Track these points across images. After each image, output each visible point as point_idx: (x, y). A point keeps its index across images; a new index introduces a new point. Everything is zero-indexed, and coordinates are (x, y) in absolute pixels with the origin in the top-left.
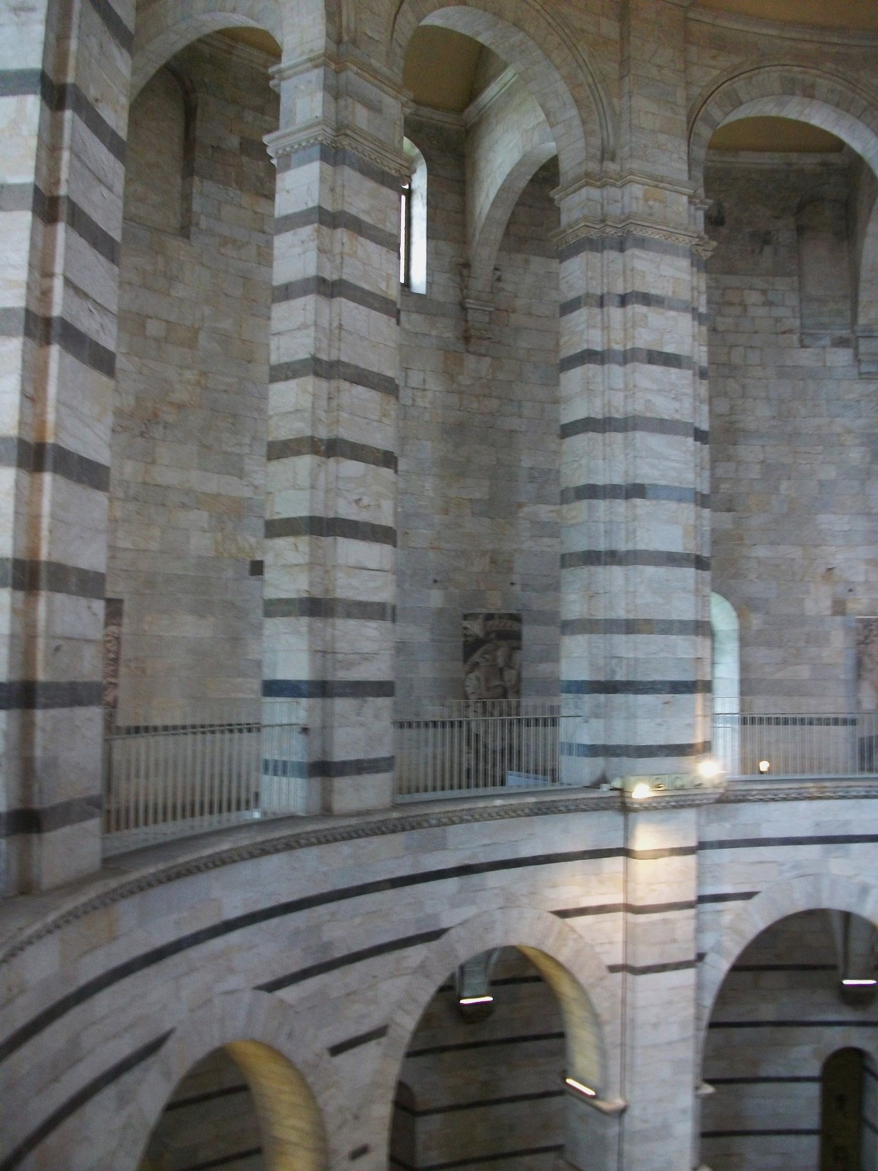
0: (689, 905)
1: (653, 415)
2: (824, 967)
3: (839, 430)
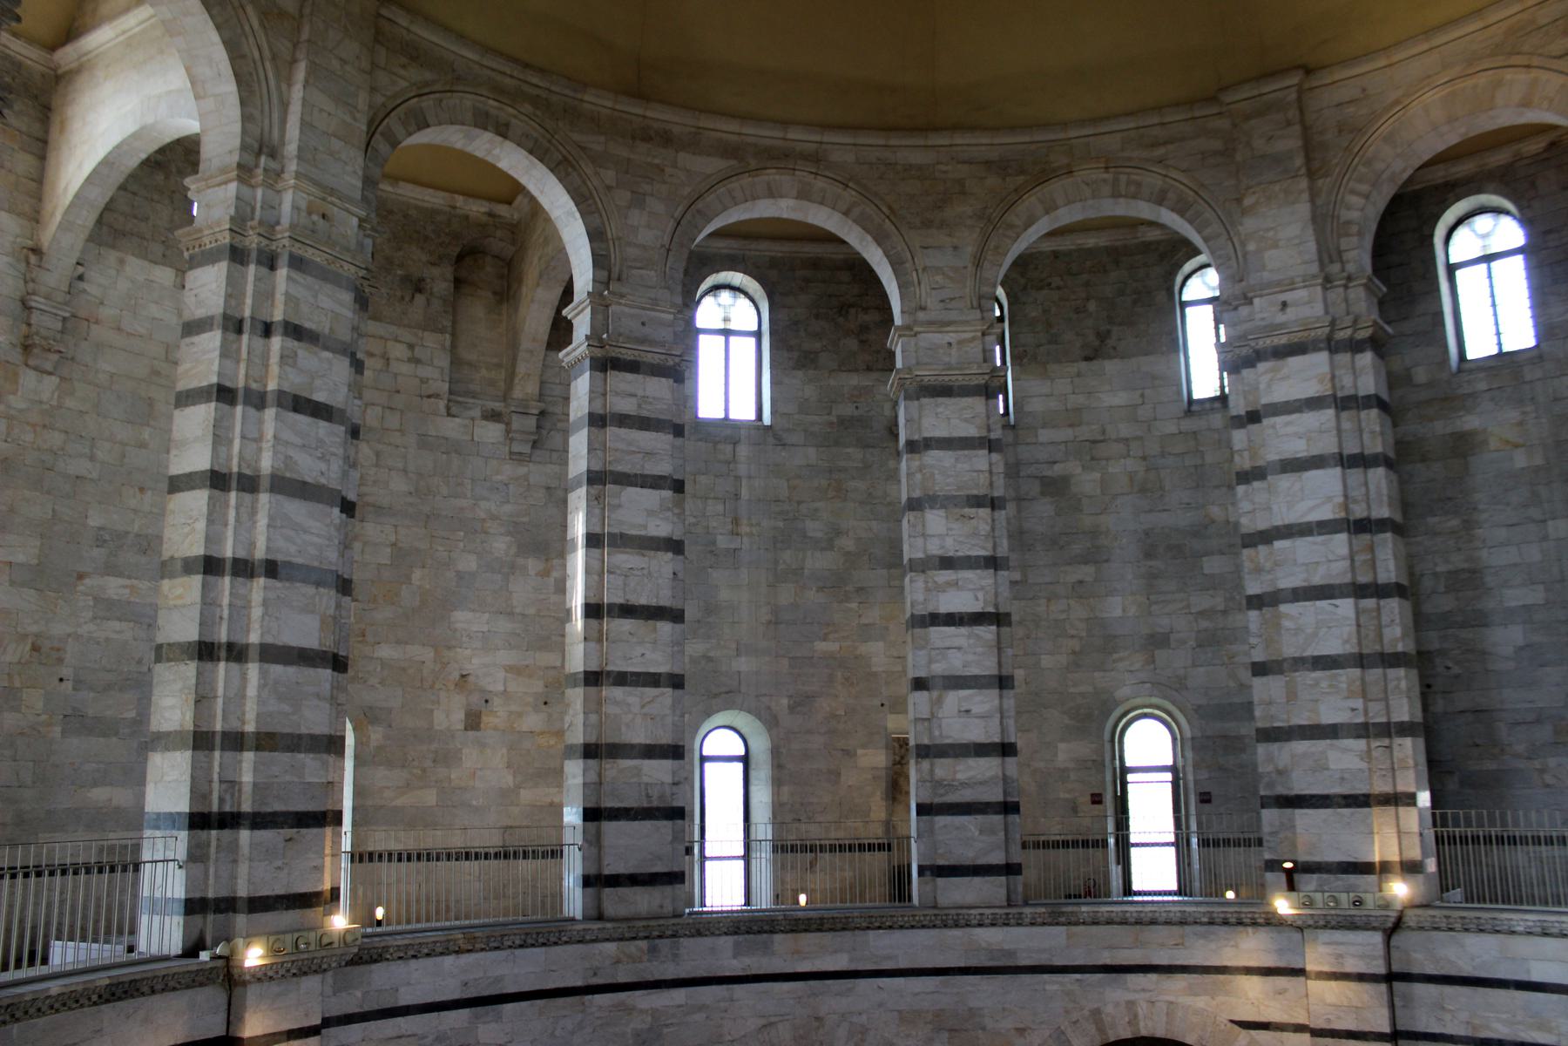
1: (295, 476)
3: (483, 515)
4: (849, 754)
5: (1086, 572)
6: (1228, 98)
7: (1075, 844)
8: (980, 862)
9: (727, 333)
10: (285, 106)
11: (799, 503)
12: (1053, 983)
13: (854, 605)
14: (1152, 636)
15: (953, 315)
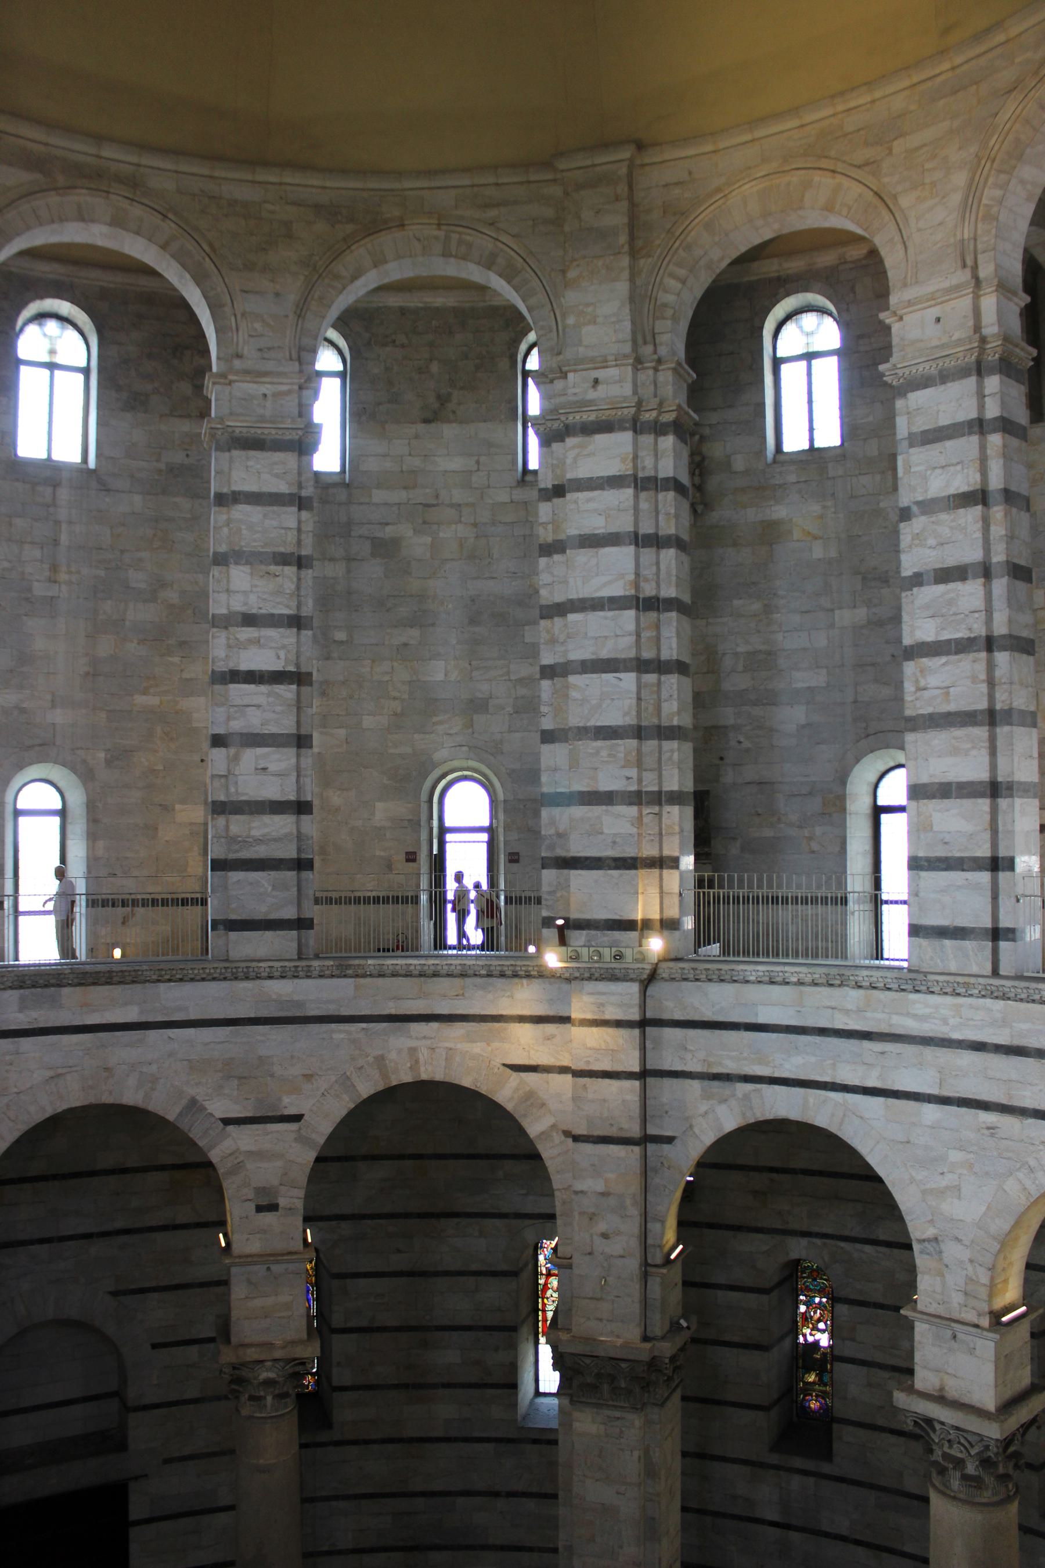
4: (167, 809)
5: (413, 635)
6: (562, 165)
7: (386, 900)
8: (274, 916)
9: (52, 366)
11: (122, 552)
12: (340, 1032)
13: (176, 660)
14: (472, 701)
15: (270, 366)
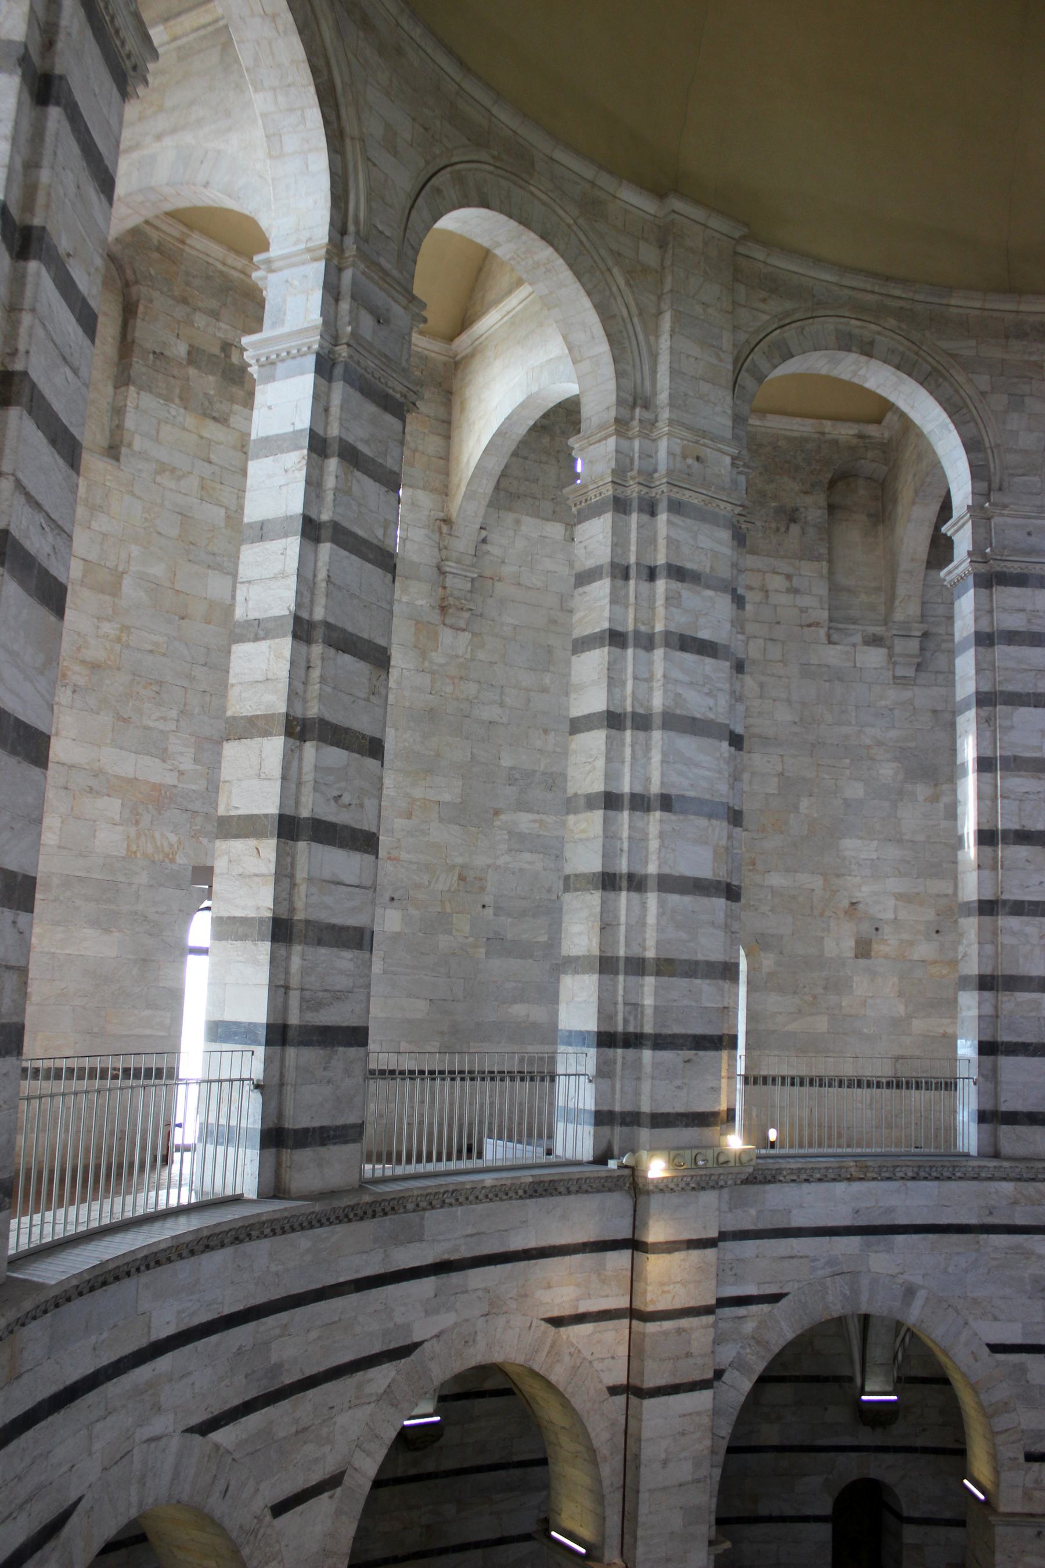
0: (708, 1310)
1: (684, 713)
2: (837, 1379)
3: (868, 742)
10: (654, 357)
